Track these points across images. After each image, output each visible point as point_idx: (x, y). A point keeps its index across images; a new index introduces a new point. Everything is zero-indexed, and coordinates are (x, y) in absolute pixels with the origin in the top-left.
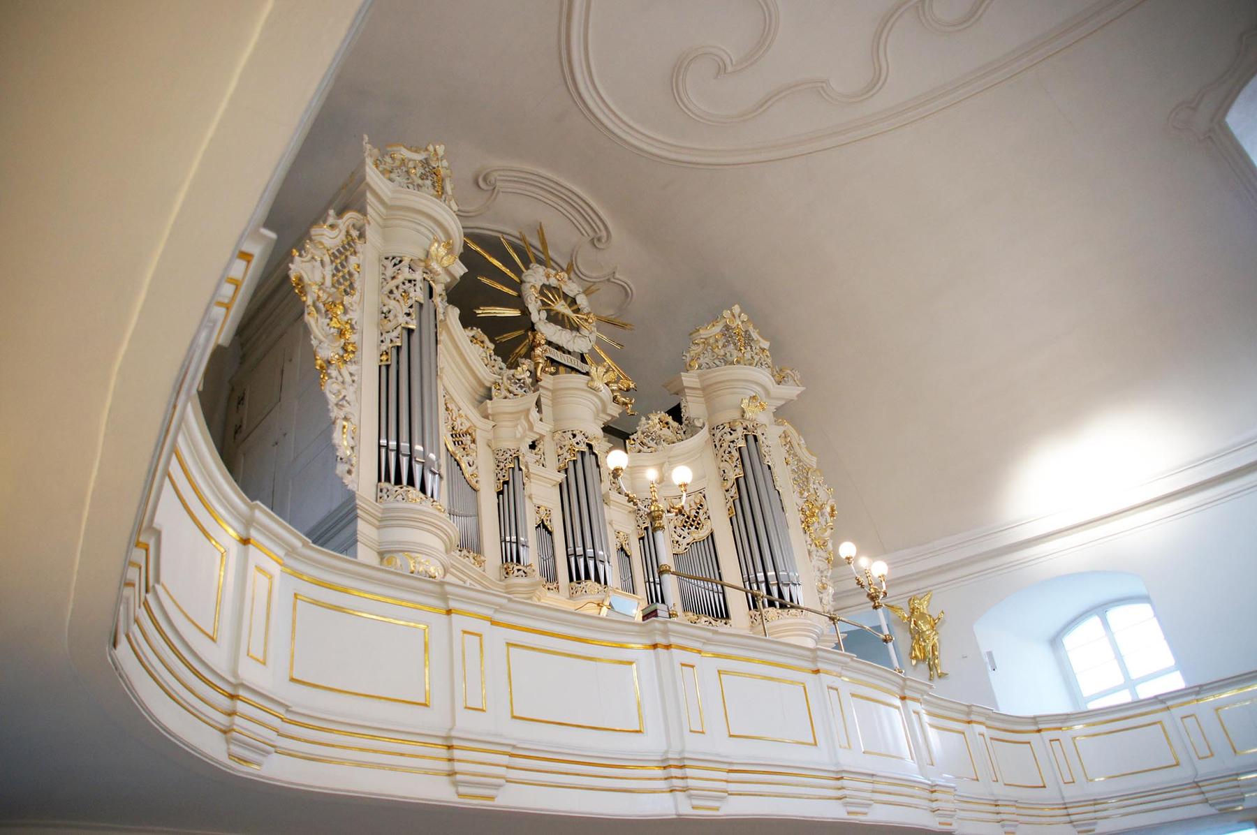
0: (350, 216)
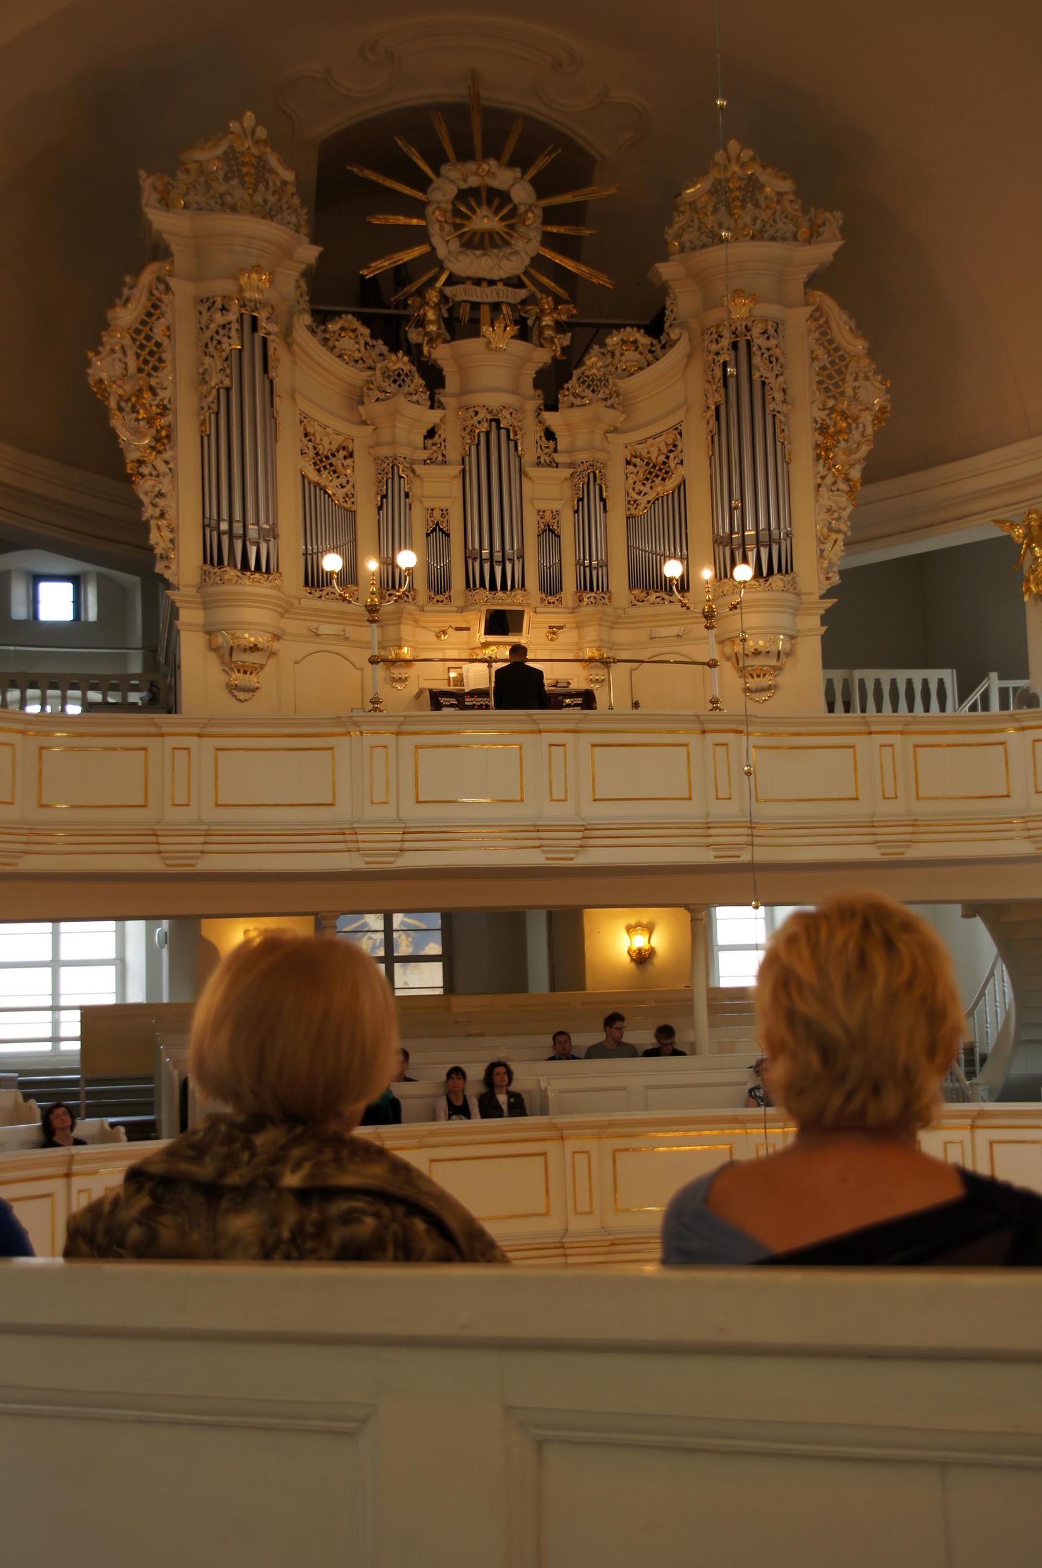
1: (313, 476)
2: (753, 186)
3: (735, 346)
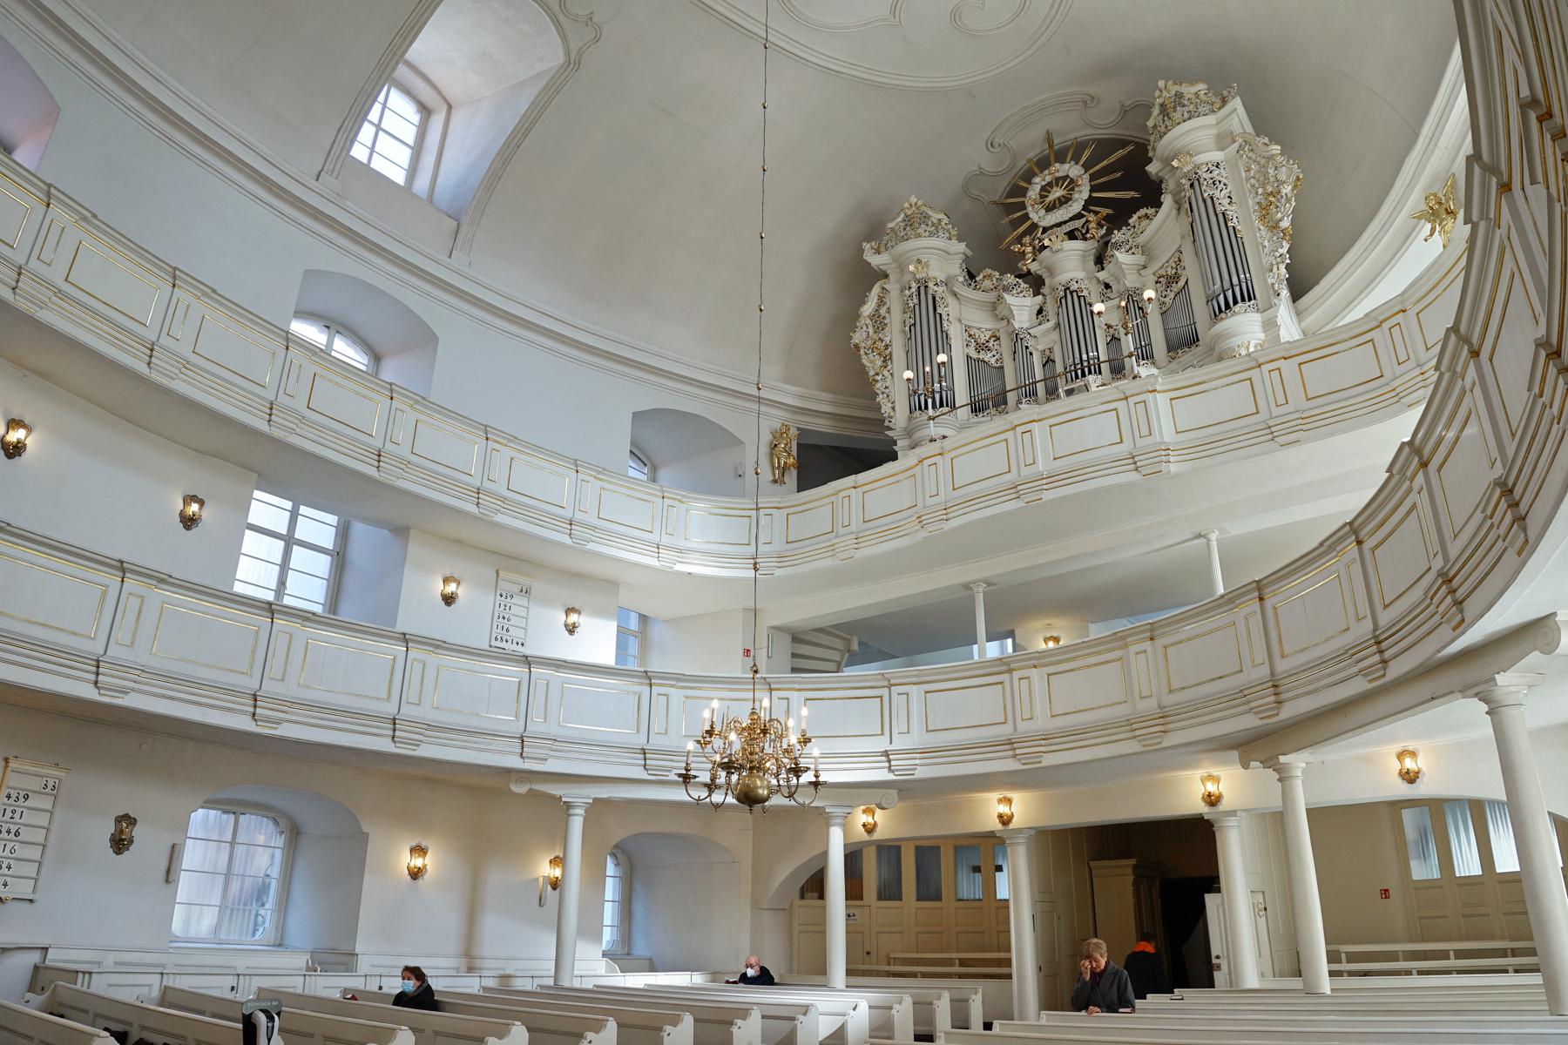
0: (876, 290)
1: (974, 355)
2: (1179, 95)
3: (1192, 185)
